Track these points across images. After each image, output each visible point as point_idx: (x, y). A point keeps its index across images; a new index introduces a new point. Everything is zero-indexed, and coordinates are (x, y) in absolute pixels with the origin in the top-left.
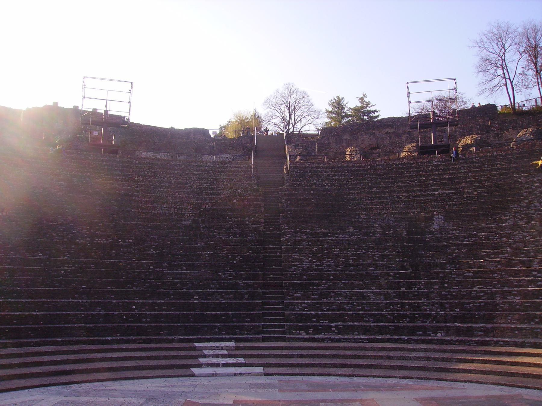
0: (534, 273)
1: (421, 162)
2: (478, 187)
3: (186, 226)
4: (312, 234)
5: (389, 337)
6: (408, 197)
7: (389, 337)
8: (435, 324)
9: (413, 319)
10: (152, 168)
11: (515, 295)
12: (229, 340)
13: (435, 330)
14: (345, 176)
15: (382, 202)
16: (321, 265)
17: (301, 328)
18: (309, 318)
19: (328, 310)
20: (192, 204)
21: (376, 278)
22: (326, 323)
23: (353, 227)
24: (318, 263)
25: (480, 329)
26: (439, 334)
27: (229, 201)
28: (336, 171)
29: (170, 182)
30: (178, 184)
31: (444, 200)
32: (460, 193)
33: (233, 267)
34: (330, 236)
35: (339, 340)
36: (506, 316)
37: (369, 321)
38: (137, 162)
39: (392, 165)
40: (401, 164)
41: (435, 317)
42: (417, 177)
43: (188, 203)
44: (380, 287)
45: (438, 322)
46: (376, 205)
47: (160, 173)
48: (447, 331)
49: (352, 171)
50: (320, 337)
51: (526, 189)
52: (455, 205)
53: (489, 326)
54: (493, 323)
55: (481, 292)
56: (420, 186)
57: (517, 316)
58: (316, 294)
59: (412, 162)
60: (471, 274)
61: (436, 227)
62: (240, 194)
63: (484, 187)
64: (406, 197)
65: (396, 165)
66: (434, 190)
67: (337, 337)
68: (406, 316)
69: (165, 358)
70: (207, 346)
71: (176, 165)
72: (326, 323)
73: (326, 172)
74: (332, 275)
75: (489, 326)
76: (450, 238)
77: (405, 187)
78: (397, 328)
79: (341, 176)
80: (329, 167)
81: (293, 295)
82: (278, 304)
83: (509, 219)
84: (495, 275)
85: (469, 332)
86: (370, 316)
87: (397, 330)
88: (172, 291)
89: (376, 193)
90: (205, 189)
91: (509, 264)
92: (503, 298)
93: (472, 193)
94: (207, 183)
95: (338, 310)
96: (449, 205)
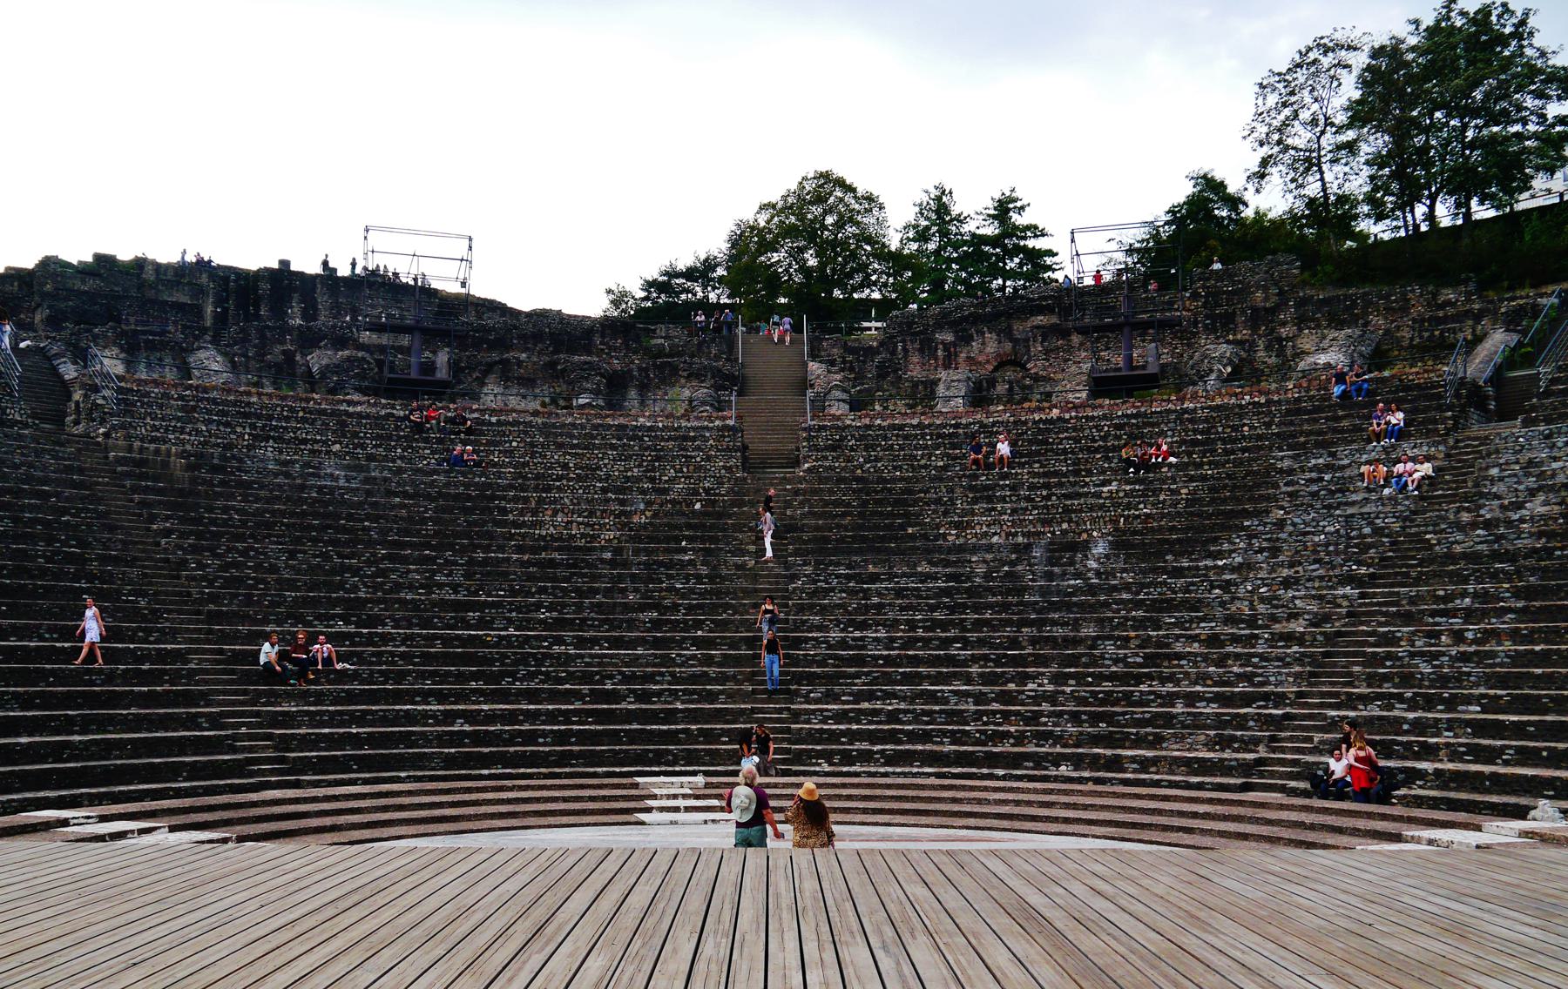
0: (1255, 660)
1: (1087, 418)
2: (1192, 479)
3: (603, 561)
4: (849, 578)
5: (974, 770)
6: (1048, 498)
7: (974, 770)
8: (1058, 749)
9: (1020, 739)
10: (526, 433)
11: (1209, 701)
12: (694, 774)
13: (1057, 760)
14: (926, 447)
15: (994, 509)
16: (862, 639)
17: (820, 754)
18: (834, 737)
19: (871, 722)
20: (612, 512)
21: (964, 663)
22: (865, 746)
23: (931, 563)
24: (857, 634)
25: (1133, 759)
26: (1063, 768)
27: (688, 506)
28: (906, 437)
29: (565, 466)
30: (581, 468)
31: (1116, 505)
32: (1154, 491)
33: (697, 642)
34: (882, 581)
35: (886, 775)
36: (1183, 737)
37: (942, 743)
38: (494, 419)
39: (1025, 423)
40: (1046, 422)
41: (1061, 737)
42: (1073, 453)
43: (604, 511)
44: (968, 680)
45: (1065, 746)
46: (982, 514)
47: (543, 445)
48: (1077, 762)
49: (939, 436)
50: (852, 769)
51: (1286, 484)
52: (1138, 516)
53: (1150, 754)
54: (1162, 749)
55: (1150, 693)
56: (1077, 473)
57: (1202, 737)
58: (850, 694)
59: (1067, 416)
60: (1139, 660)
61: (1092, 564)
62: (707, 491)
63: (1204, 478)
64: (1044, 498)
65: (1035, 422)
66: (1104, 484)
67: (882, 770)
68: (1007, 734)
69: (565, 800)
70: (660, 785)
71: (573, 425)
72: (865, 746)
73: (885, 438)
74: (881, 657)
75: (1150, 754)
76: (1115, 588)
77: (1045, 475)
78: (989, 755)
79: (916, 449)
80: (893, 427)
81: (806, 696)
82: (780, 711)
83: (1234, 551)
84: (1183, 662)
85: (1115, 764)
86: (944, 733)
87: (993, 760)
88: (585, 688)
89: (986, 488)
90: (638, 479)
91: (1213, 640)
92: (1187, 706)
93: (1176, 492)
94: (640, 466)
95: (888, 723)
96: (1127, 518)
